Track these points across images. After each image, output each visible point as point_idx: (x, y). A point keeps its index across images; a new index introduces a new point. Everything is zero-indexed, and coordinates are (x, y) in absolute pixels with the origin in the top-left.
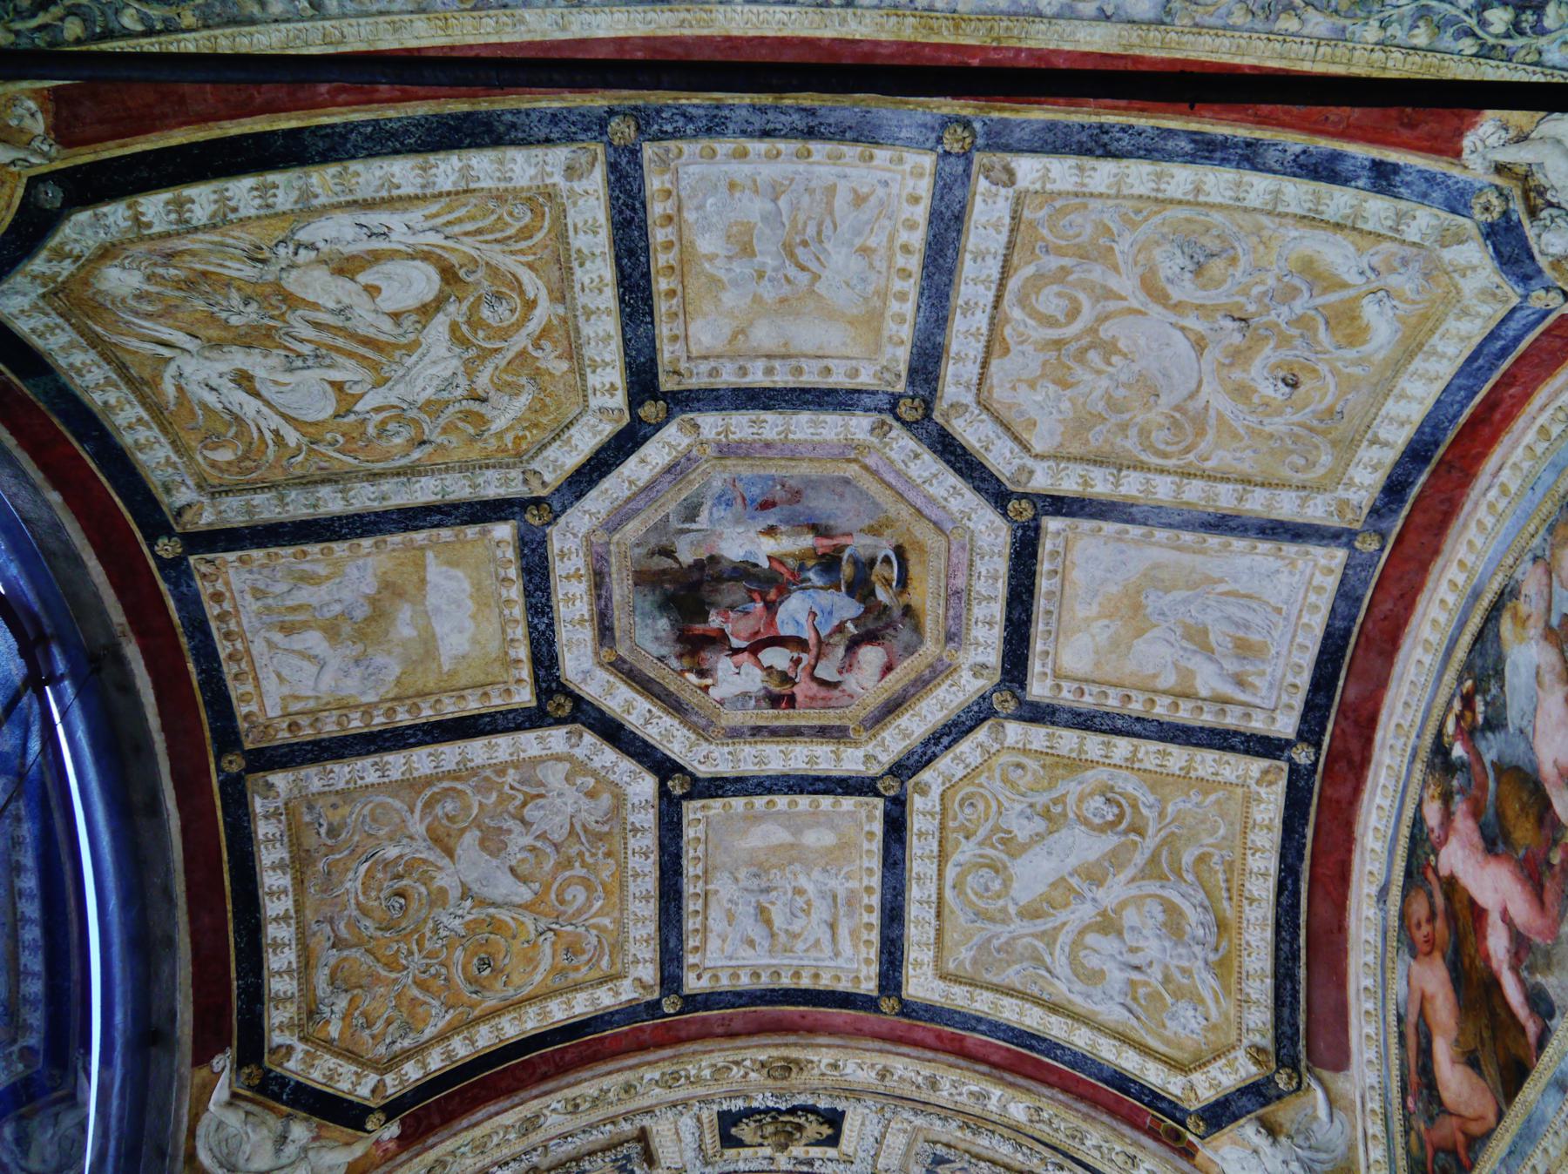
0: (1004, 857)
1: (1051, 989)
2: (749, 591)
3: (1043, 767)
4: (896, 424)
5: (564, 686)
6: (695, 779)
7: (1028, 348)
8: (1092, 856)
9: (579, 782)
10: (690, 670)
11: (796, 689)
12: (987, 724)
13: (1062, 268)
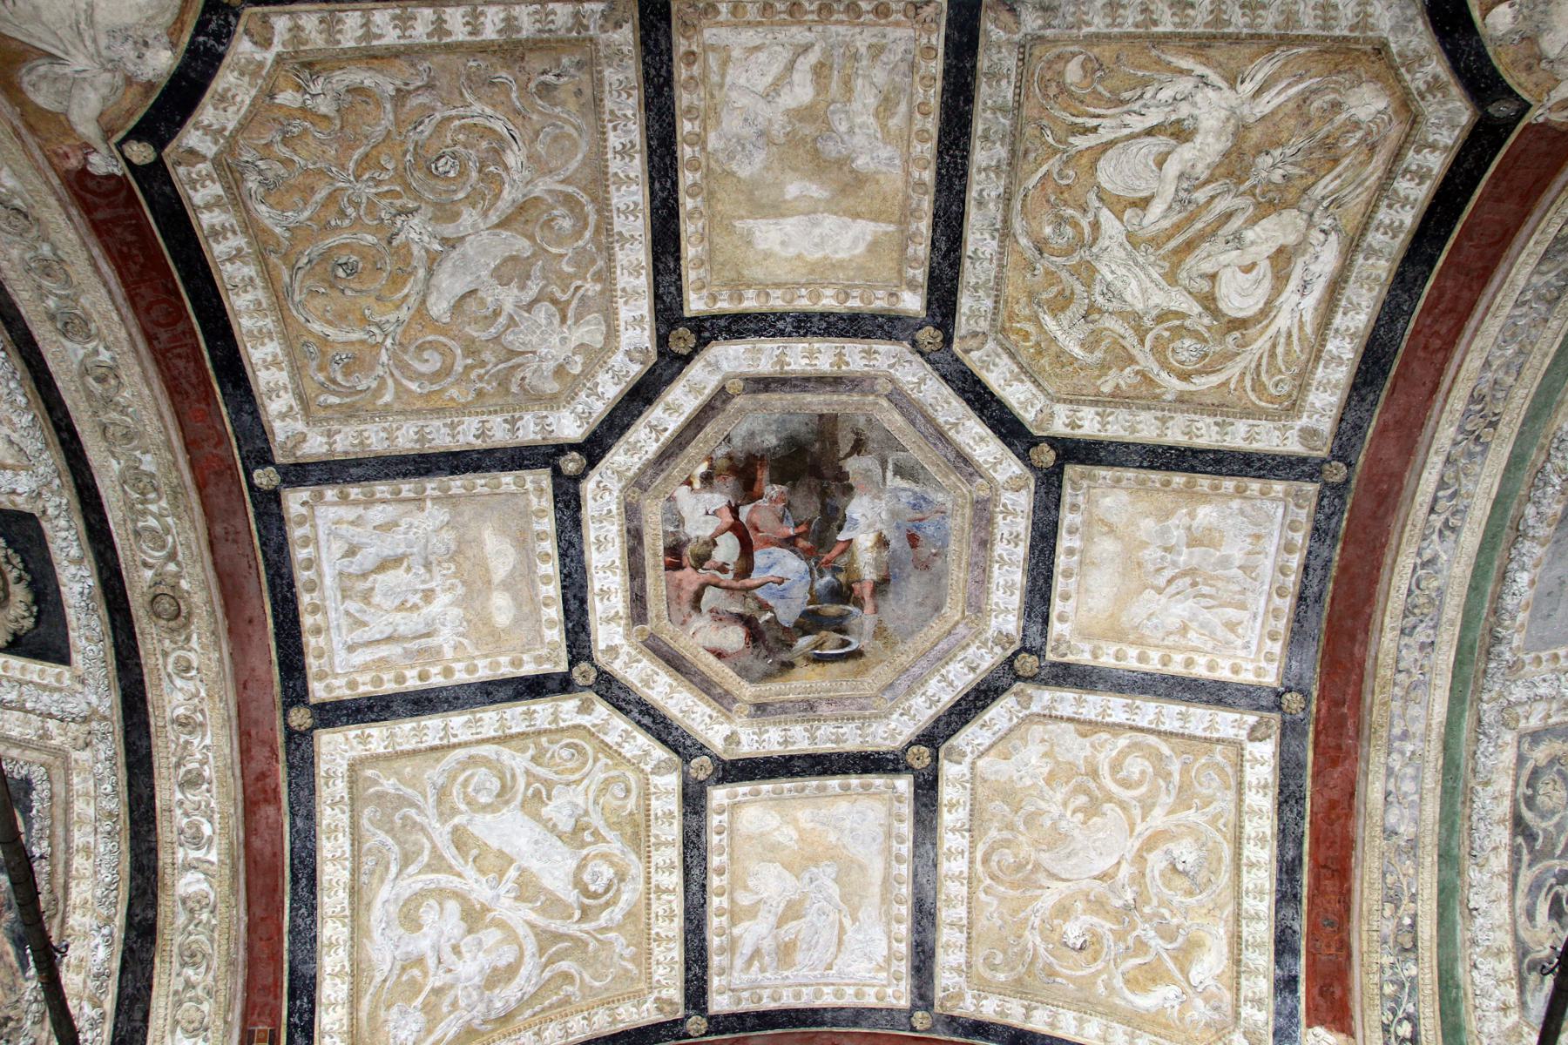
0: (520, 797)
1: (375, 881)
2: (809, 523)
3: (631, 814)
4: (1009, 653)
5: (706, 344)
7: (1088, 751)
8: (548, 882)
9: (578, 358)
10: (711, 467)
11: (689, 570)
12: (675, 757)
13: (1170, 774)
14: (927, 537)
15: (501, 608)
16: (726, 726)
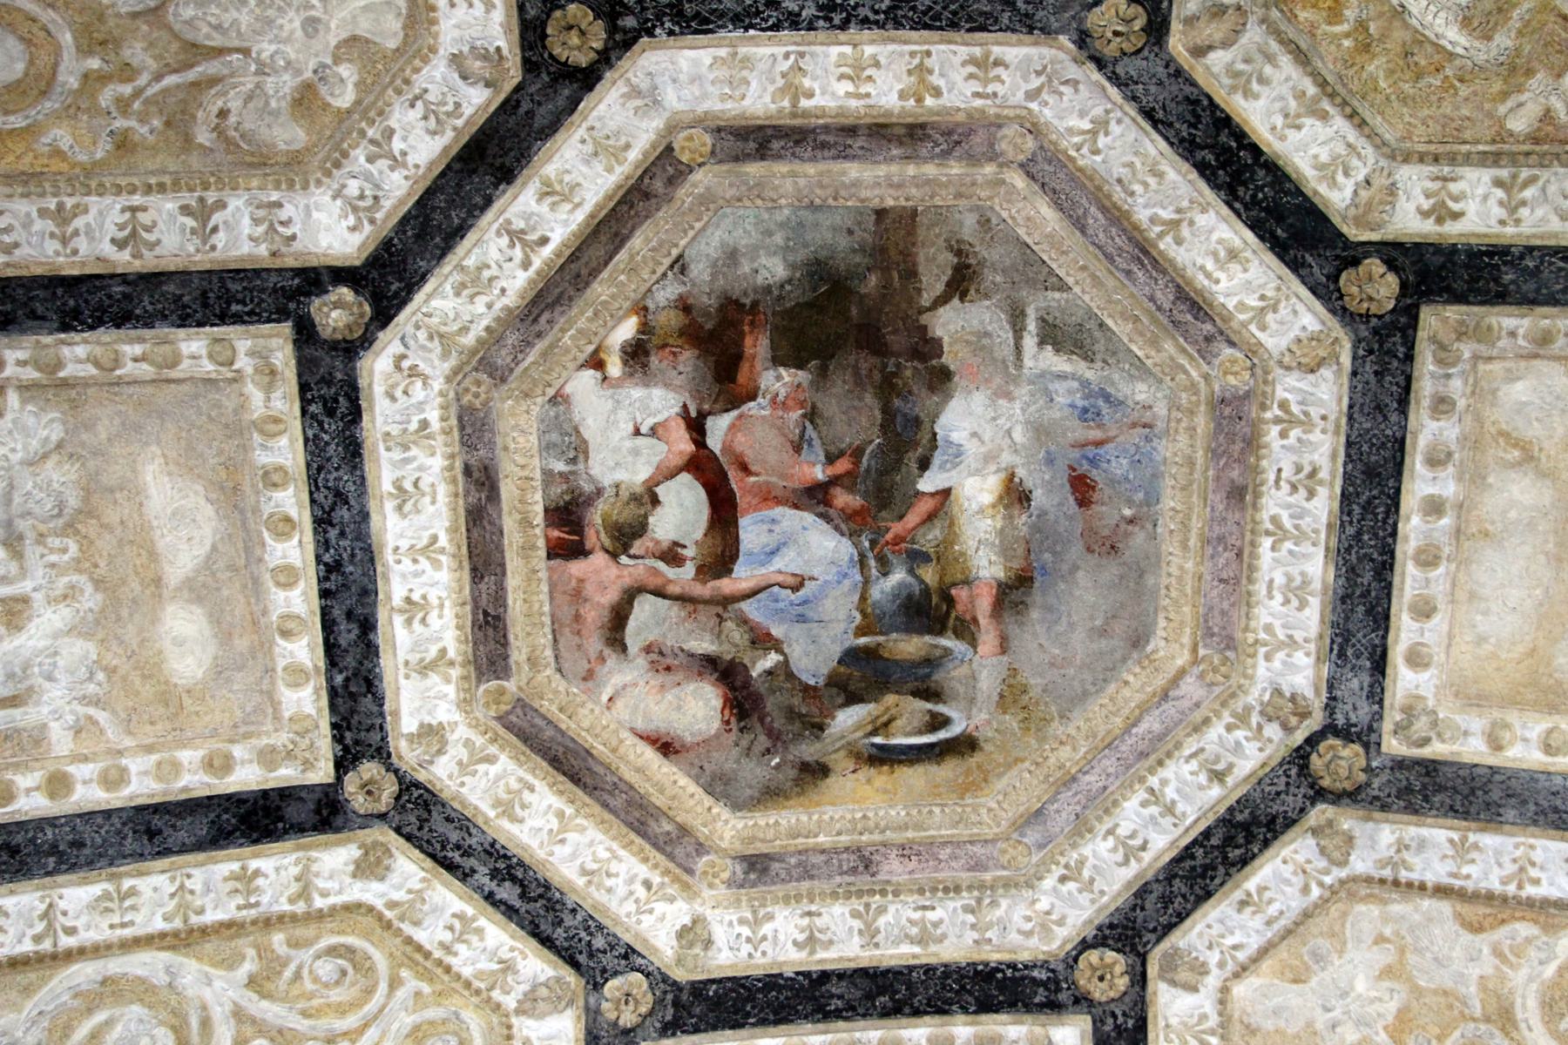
2: (858, 453)
4: (1299, 737)
6: (352, 348)
7: (1488, 965)
9: (345, 70)
10: (645, 328)
11: (599, 559)
12: (570, 977)
14: (1112, 482)
15: (185, 641)
16: (681, 904)
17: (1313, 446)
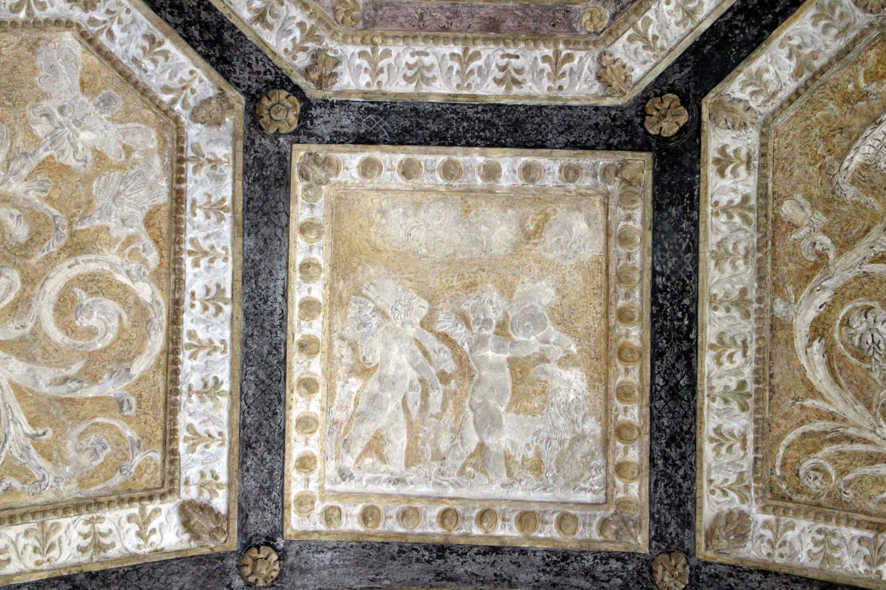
4: (300, 81)
7: (120, 233)
13: (95, 379)
17: (537, 82)
